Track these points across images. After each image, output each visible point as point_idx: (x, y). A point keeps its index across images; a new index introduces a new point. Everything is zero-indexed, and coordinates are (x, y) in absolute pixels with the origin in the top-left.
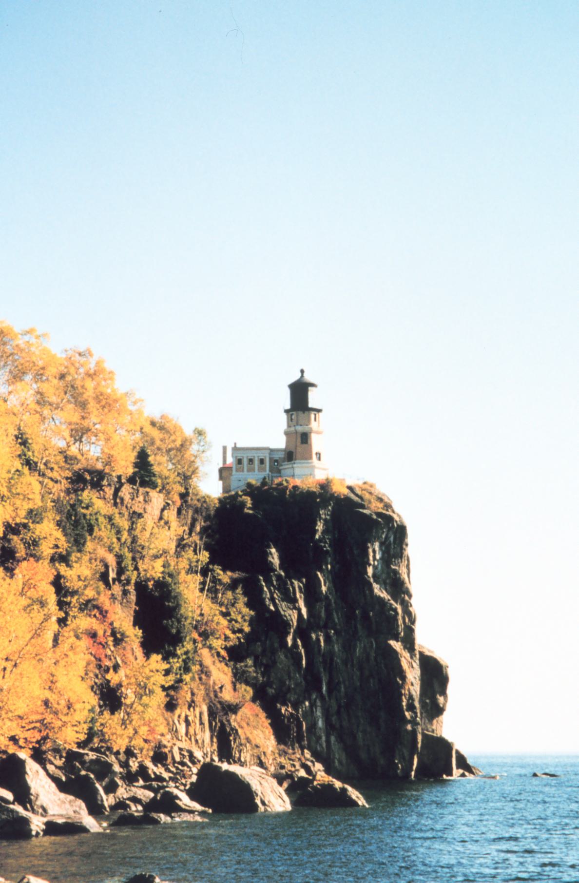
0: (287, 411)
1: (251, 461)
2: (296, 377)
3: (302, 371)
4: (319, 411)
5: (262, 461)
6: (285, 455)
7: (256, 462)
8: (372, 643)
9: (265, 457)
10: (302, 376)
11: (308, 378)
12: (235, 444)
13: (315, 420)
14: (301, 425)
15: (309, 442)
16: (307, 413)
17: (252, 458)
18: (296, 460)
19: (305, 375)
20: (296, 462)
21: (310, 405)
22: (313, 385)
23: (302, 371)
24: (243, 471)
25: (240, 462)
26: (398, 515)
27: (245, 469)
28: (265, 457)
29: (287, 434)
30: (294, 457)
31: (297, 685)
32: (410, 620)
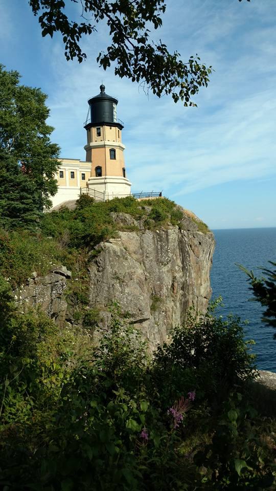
2: (96, 93)
3: (102, 88)
11: (108, 92)
18: (106, 175)
20: (107, 177)
23: (102, 88)
30: (103, 173)
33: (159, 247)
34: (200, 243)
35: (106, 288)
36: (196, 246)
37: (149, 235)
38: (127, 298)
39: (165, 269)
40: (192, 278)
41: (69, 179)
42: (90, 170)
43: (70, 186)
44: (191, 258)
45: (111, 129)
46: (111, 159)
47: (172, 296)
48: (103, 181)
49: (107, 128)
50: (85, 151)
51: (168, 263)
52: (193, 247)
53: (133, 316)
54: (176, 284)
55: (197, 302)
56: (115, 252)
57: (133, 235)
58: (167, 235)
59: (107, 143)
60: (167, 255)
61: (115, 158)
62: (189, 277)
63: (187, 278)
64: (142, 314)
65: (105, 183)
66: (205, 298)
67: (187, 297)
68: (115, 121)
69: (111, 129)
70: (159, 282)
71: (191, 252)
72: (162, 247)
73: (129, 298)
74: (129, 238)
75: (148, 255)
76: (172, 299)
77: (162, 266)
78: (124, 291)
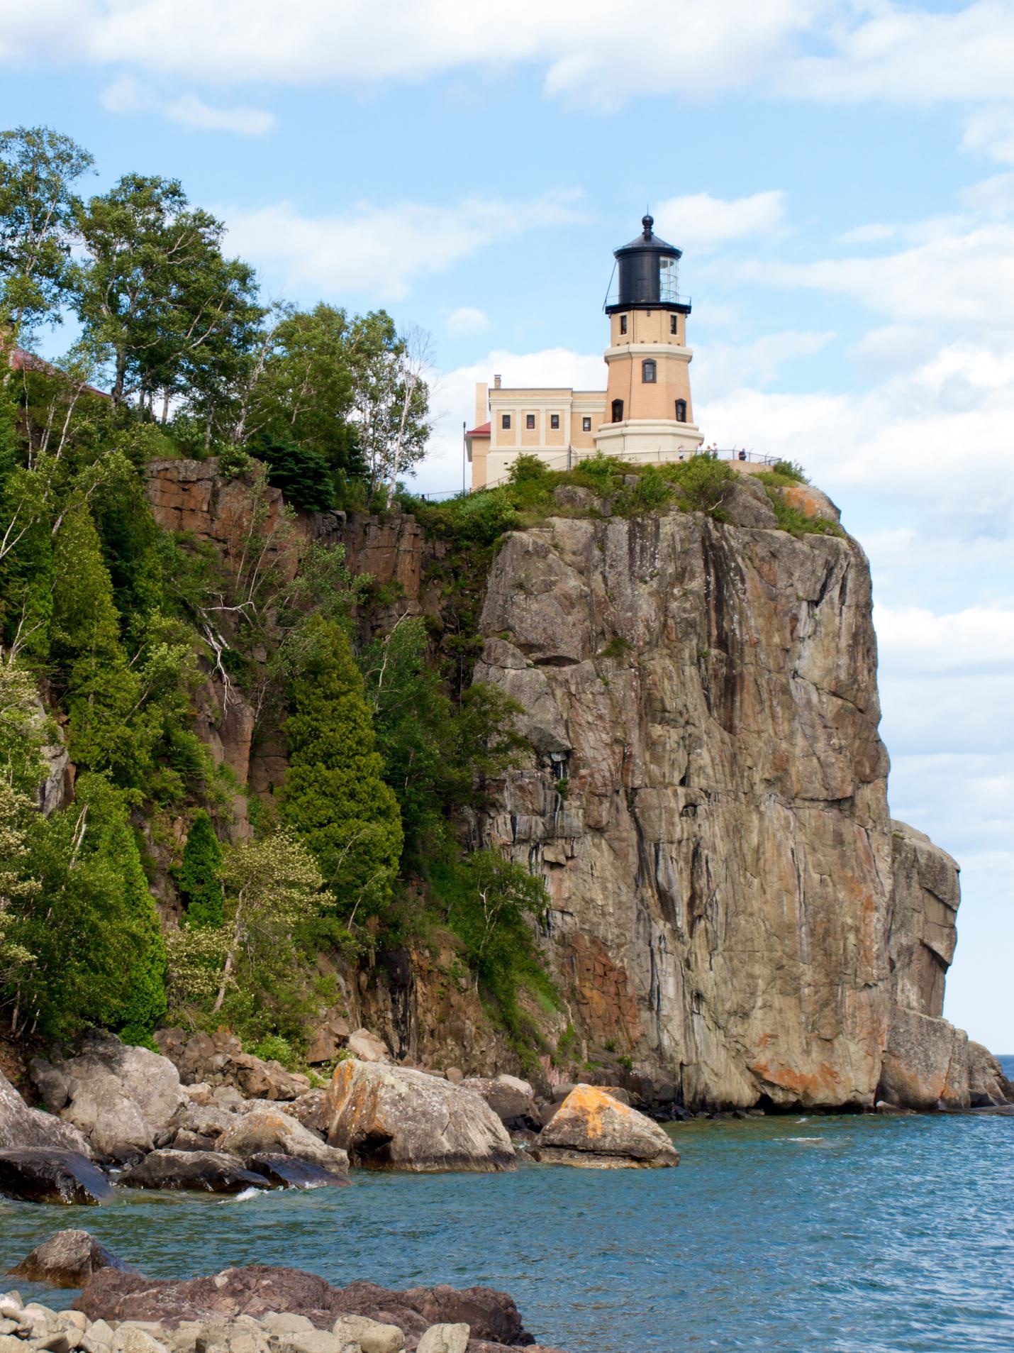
0: (611, 310)
1: (531, 421)
2: (632, 235)
3: (648, 223)
4: (685, 310)
7: (543, 422)
8: (786, 818)
10: (648, 235)
11: (662, 233)
12: (498, 379)
13: (674, 331)
16: (654, 314)
19: (654, 229)
22: (674, 253)
23: (648, 223)
24: (513, 442)
25: (506, 422)
26: (852, 543)
28: (562, 410)
29: (607, 360)
31: (620, 905)
32: (873, 770)
33: (638, 549)
34: (773, 555)
36: (762, 559)
37: (620, 529)
39: (643, 589)
40: (749, 628)
43: (547, 443)
44: (748, 585)
46: (645, 381)
47: (668, 647)
48: (618, 431)
49: (641, 315)
52: (757, 563)
53: (540, 648)
54: (670, 622)
55: (768, 684)
56: (523, 545)
57: (585, 526)
58: (658, 527)
59: (635, 347)
60: (652, 564)
61: (654, 381)
62: (740, 623)
63: (736, 626)
64: (555, 647)
65: (623, 435)
66: (835, 694)
67: (739, 669)
68: (664, 298)
70: (630, 614)
71: (750, 573)
72: (643, 549)
73: (536, 619)
74: (571, 528)
76: (665, 651)
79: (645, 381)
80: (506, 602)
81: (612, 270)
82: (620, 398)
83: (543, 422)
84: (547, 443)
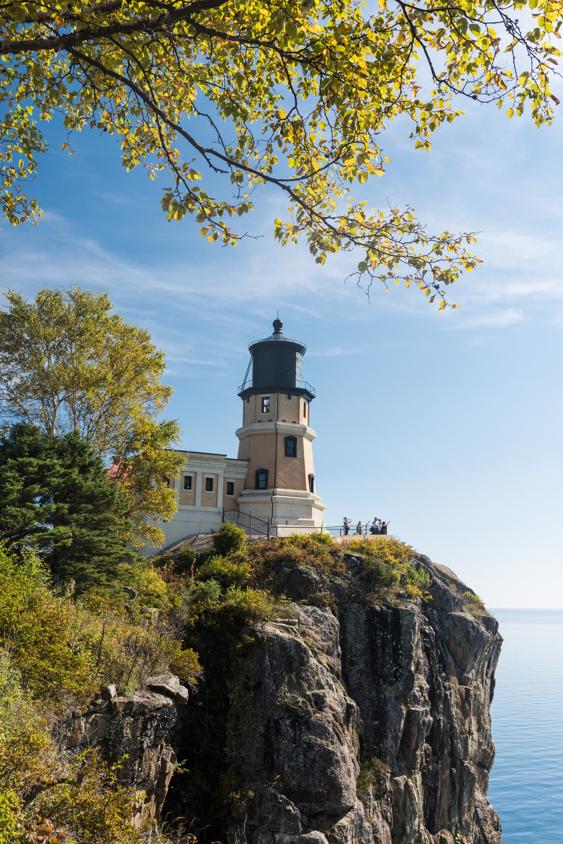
2: (267, 333)
3: (277, 325)
5: (209, 484)
6: (247, 475)
7: (199, 484)
9: (217, 475)
14: (284, 421)
15: (298, 453)
16: (294, 398)
17: (191, 475)
18: (275, 487)
21: (298, 385)
23: (277, 325)
27: (198, 501)
28: (217, 475)
29: (239, 434)
30: (271, 482)
35: (261, 729)
38: (305, 755)
41: (203, 492)
42: (243, 477)
45: (289, 398)
46: (287, 455)
50: (237, 439)
51: (397, 680)
61: (294, 455)
68: (298, 385)
69: (289, 398)
70: (376, 723)
75: (354, 659)
77: (385, 686)
78: (300, 737)
79: (287, 455)
80: (267, 727)
81: (248, 356)
82: (265, 467)
83: (199, 484)
84: (203, 505)
